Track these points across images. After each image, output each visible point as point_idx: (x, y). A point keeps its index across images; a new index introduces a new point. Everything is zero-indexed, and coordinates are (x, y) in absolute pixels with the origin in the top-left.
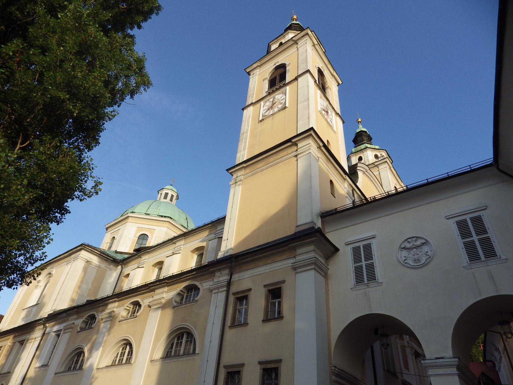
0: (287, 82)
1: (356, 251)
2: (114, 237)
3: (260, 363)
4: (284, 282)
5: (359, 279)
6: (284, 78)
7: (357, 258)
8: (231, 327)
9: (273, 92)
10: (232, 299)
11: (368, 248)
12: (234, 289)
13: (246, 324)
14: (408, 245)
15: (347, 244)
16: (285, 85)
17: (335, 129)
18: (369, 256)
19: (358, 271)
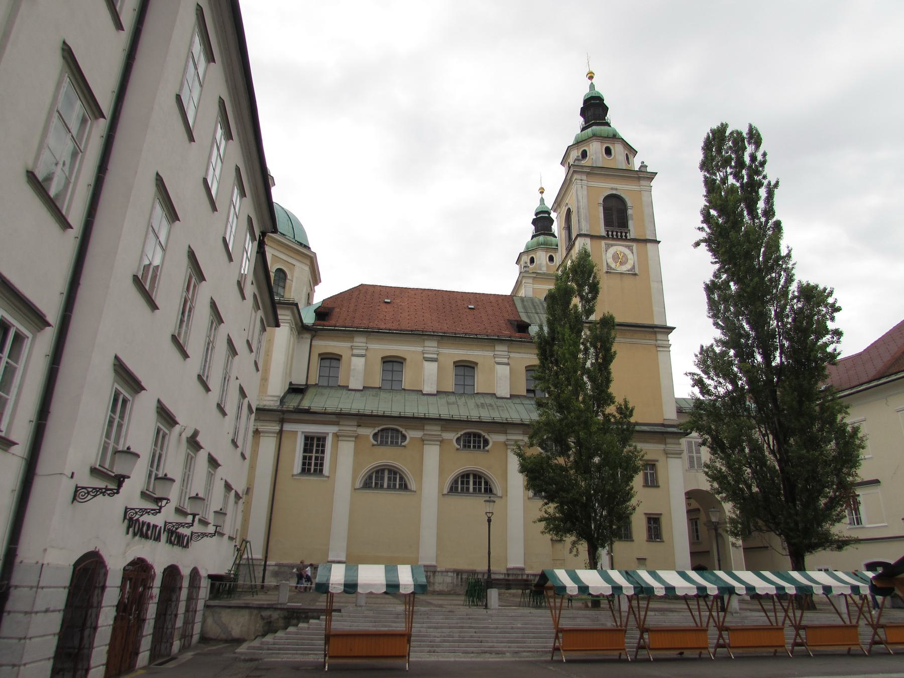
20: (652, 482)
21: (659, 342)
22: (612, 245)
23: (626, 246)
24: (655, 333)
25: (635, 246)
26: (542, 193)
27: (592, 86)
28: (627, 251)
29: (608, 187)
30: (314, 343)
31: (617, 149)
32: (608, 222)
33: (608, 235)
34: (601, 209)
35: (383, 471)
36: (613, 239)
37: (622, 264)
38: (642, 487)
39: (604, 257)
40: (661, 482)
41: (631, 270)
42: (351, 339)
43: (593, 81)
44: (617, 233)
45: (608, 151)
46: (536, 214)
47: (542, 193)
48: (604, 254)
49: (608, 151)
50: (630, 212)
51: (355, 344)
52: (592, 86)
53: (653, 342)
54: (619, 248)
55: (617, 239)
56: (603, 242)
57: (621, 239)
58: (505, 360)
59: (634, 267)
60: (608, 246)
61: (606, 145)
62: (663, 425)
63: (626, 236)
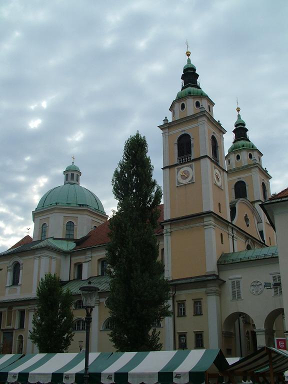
0: (192, 158)
1: (233, 283)
2: (45, 224)
3: (194, 332)
4: (202, 299)
5: (234, 297)
6: (190, 152)
7: (233, 287)
8: (178, 316)
9: (183, 164)
10: (176, 304)
11: (238, 282)
12: (177, 299)
13: (185, 315)
14: (254, 284)
15: (230, 279)
16: (190, 161)
17: (223, 189)
18: (239, 287)
19: (234, 293)
20: (198, 312)
21: (205, 223)
22: (181, 168)
23: (188, 166)
24: (203, 218)
25: (193, 163)
26: (238, 111)
27: (189, 61)
29: (178, 132)
30: (73, 259)
33: (180, 162)
35: (80, 321)
36: (182, 164)
37: (186, 178)
38: (193, 316)
39: (176, 177)
40: (203, 313)
41: (191, 180)
42: (85, 254)
43: (190, 57)
44: (185, 158)
46: (236, 126)
47: (238, 111)
48: (176, 175)
51: (87, 256)
52: (189, 61)
53: (202, 224)
54: (186, 168)
60: (179, 169)
62: (206, 276)
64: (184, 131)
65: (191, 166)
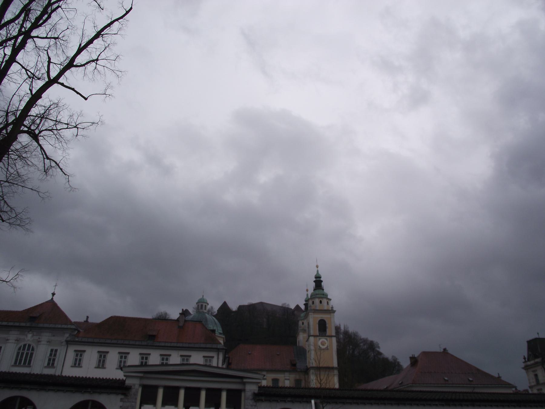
25: (328, 338)
27: (318, 271)
28: (326, 341)
31: (325, 301)
32: (320, 330)
34: (317, 325)
36: (321, 336)
45: (321, 302)
49: (321, 302)
50: (327, 325)
52: (318, 271)
54: (323, 339)
55: (323, 336)
56: (318, 338)
57: (324, 336)
58: (288, 378)
59: (327, 347)
60: (320, 339)
61: (320, 300)
63: (326, 335)
64: (322, 317)
65: (327, 340)
